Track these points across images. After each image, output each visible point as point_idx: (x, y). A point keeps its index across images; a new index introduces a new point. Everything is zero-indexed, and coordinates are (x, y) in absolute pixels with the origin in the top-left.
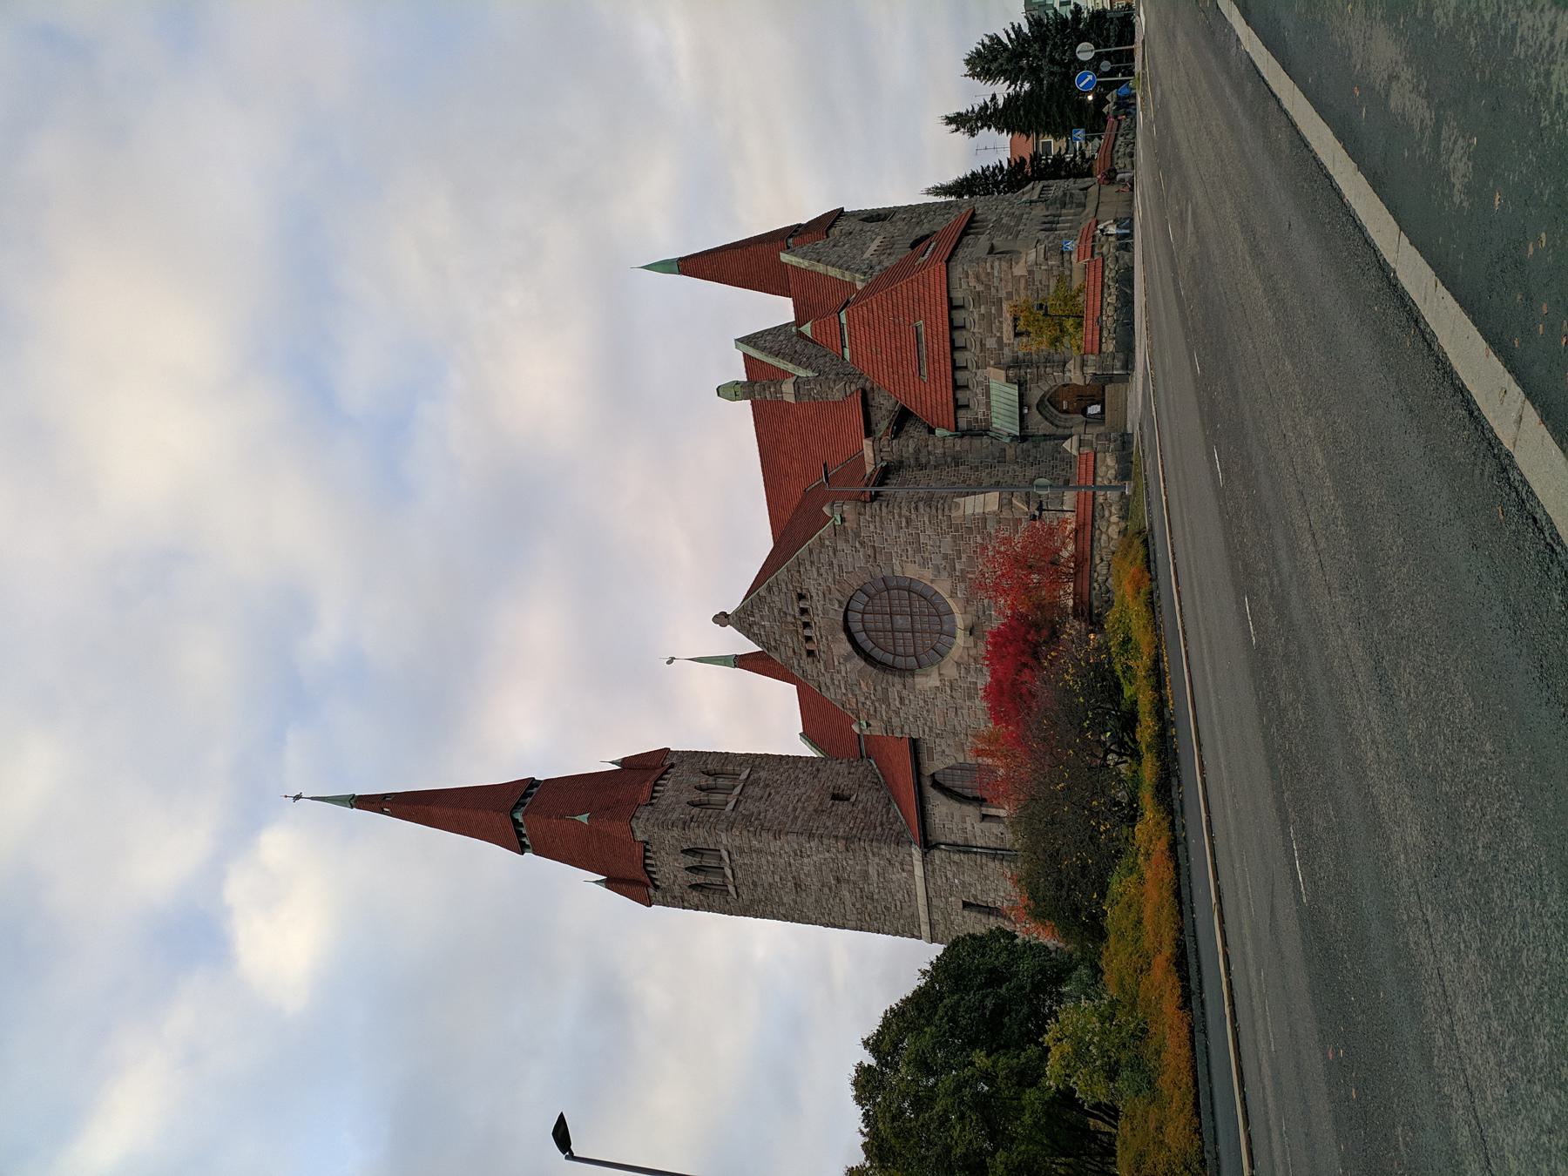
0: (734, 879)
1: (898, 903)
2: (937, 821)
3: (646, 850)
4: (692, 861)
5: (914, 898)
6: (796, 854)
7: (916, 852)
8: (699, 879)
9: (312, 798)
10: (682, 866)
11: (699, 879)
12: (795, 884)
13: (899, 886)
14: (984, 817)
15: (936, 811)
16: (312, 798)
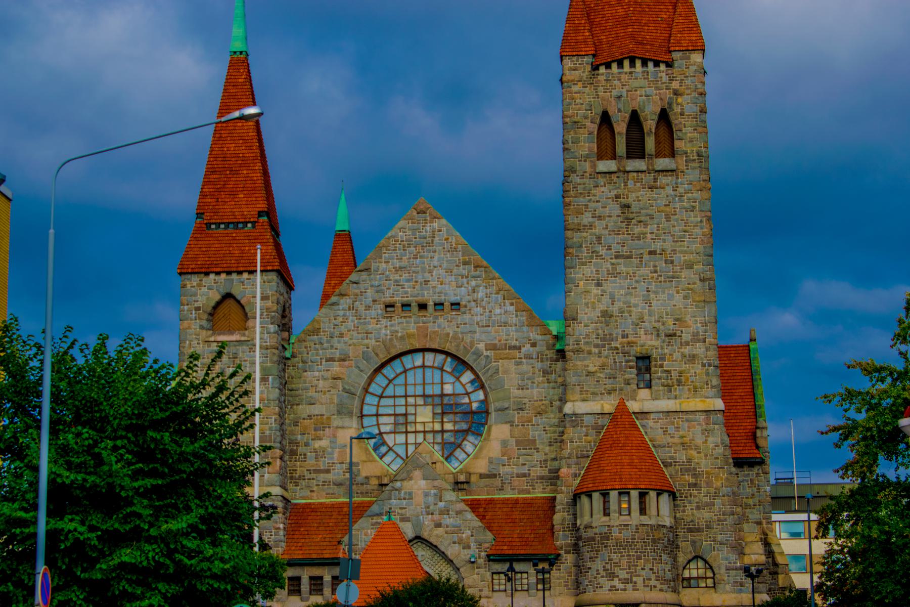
3: (657, 64)
4: (650, 124)
8: (621, 127)
11: (621, 127)
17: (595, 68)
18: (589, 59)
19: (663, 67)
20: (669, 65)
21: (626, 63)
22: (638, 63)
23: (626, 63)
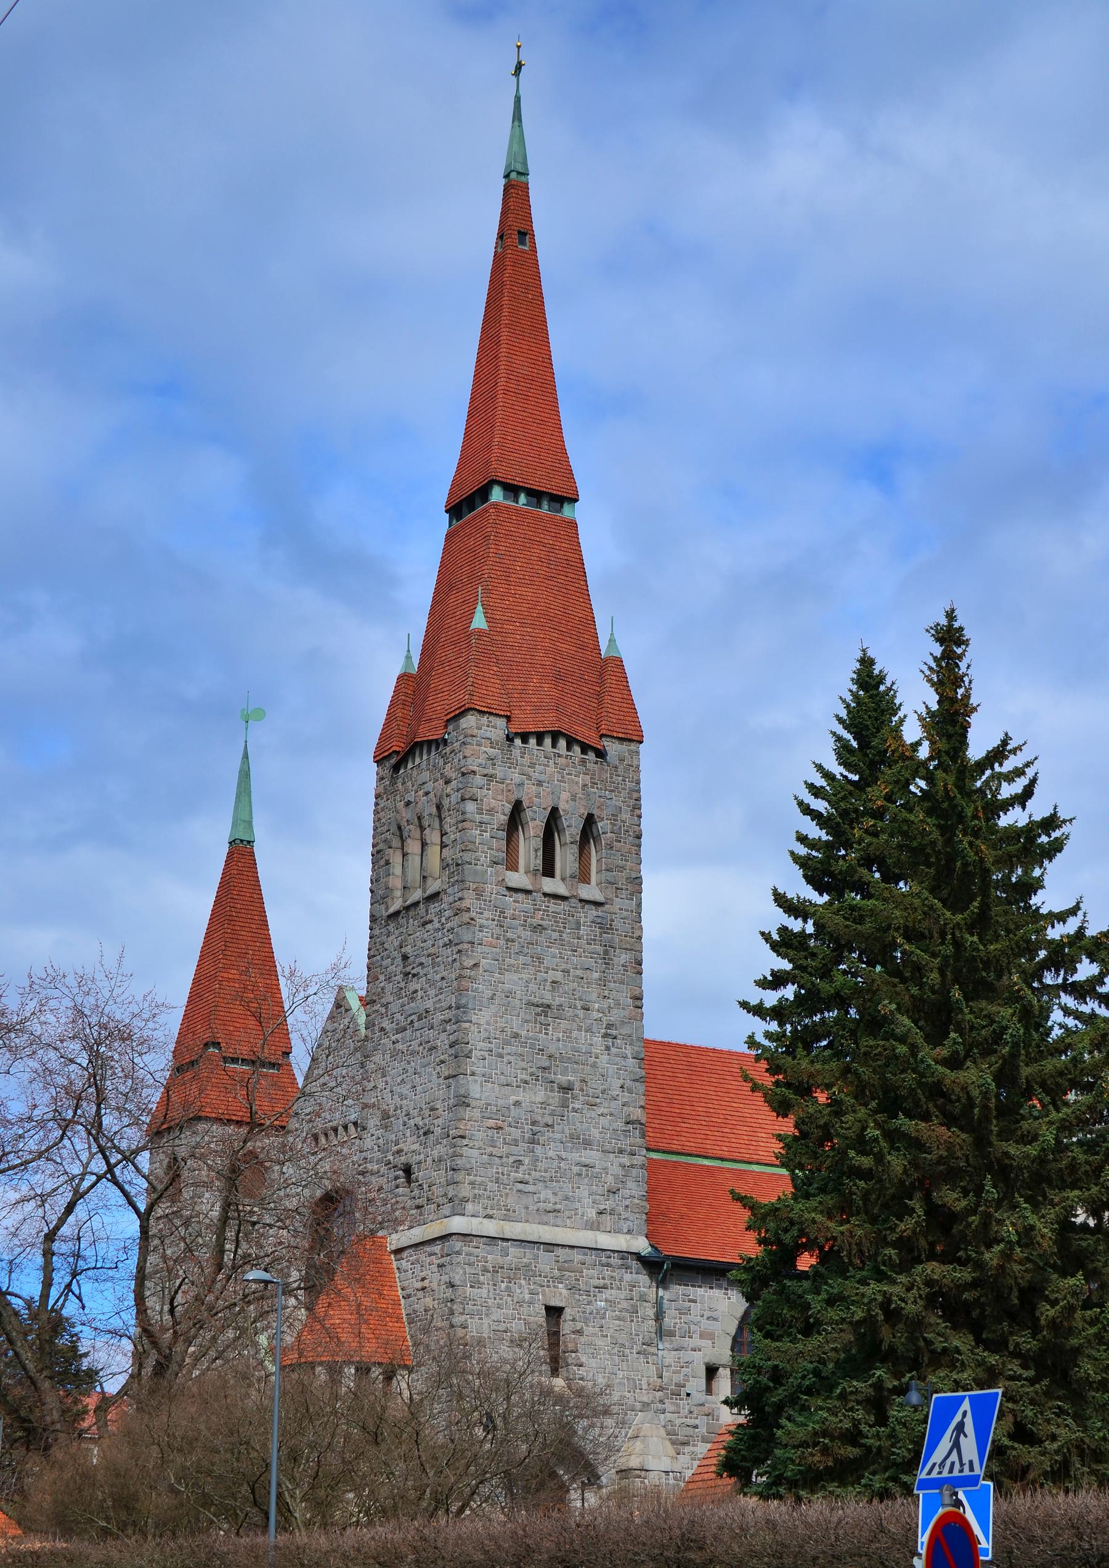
0: (545, 895)
1: (530, 1188)
2: (700, 1291)
3: (585, 748)
5: (545, 1219)
6: (609, 1026)
7: (642, 1245)
8: (535, 826)
9: (518, 100)
10: (562, 806)
12: (548, 1006)
13: (567, 1198)
14: (711, 1372)
15: (717, 1293)
16: (518, 100)
17: (510, 739)
18: (501, 723)
19: (591, 756)
20: (601, 754)
21: (548, 741)
22: (562, 743)
23: (548, 741)
